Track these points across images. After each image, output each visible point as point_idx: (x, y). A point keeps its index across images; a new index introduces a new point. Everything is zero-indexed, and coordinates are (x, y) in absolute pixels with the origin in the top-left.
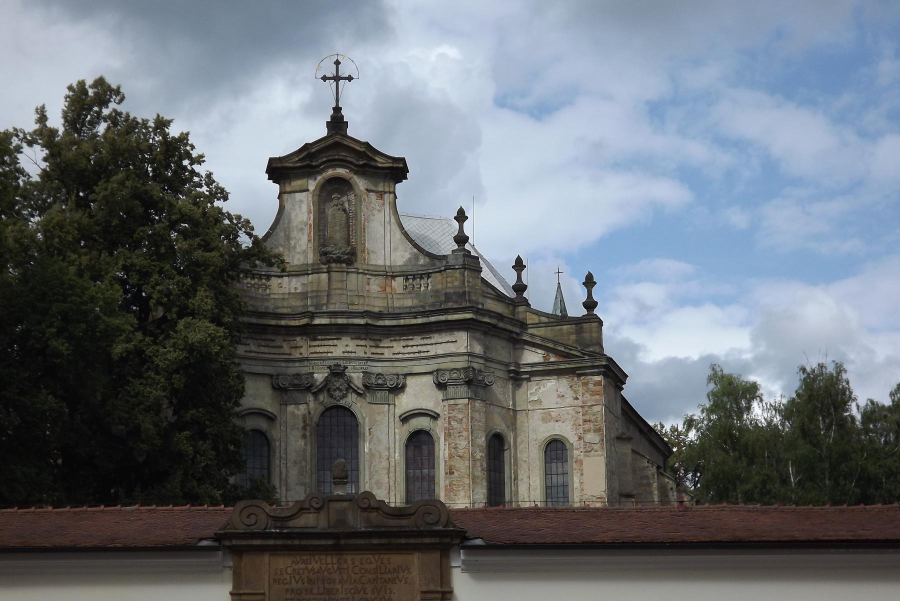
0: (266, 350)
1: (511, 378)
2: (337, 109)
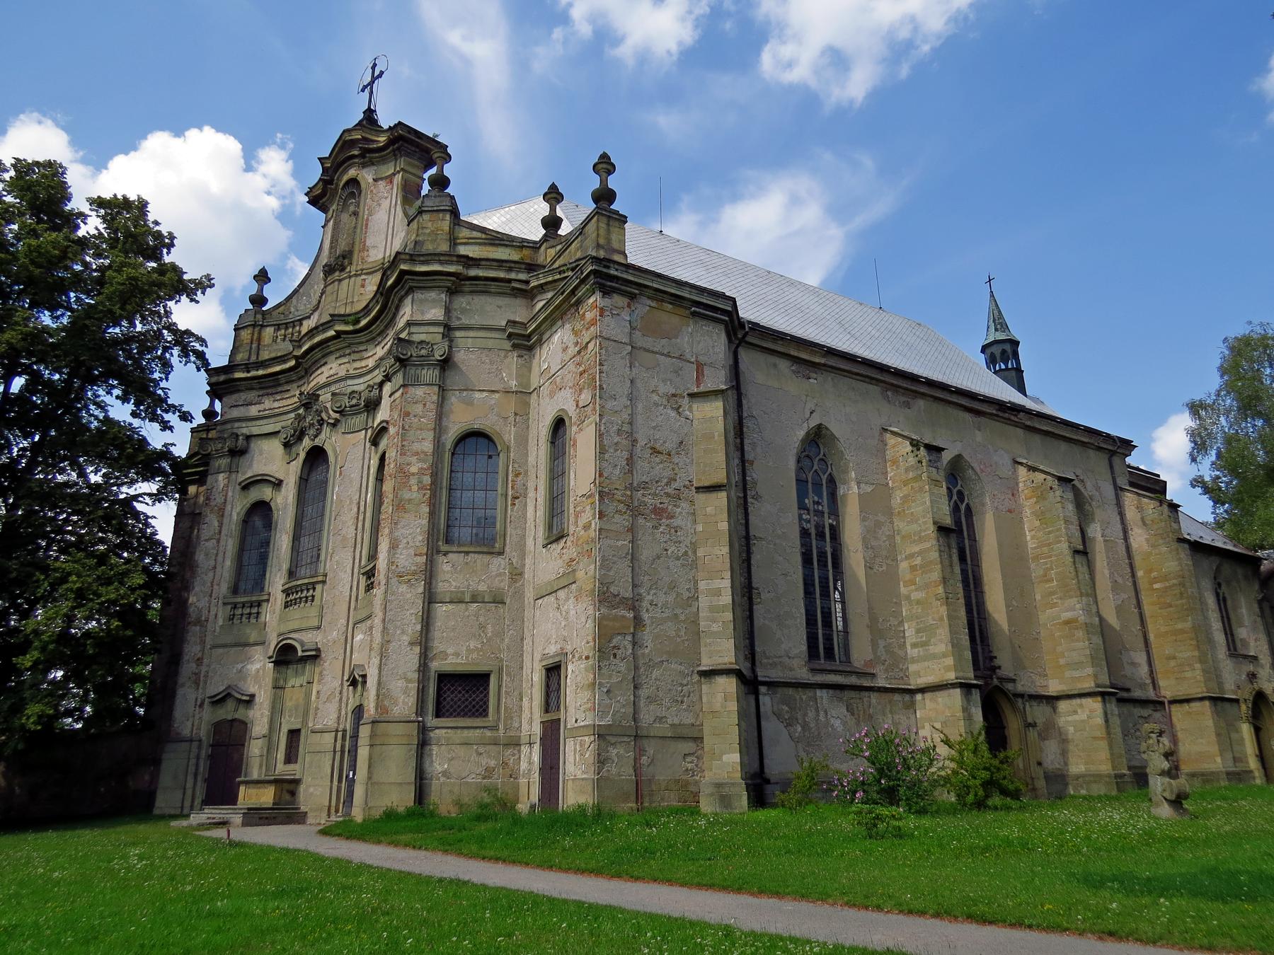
1: (515, 346)
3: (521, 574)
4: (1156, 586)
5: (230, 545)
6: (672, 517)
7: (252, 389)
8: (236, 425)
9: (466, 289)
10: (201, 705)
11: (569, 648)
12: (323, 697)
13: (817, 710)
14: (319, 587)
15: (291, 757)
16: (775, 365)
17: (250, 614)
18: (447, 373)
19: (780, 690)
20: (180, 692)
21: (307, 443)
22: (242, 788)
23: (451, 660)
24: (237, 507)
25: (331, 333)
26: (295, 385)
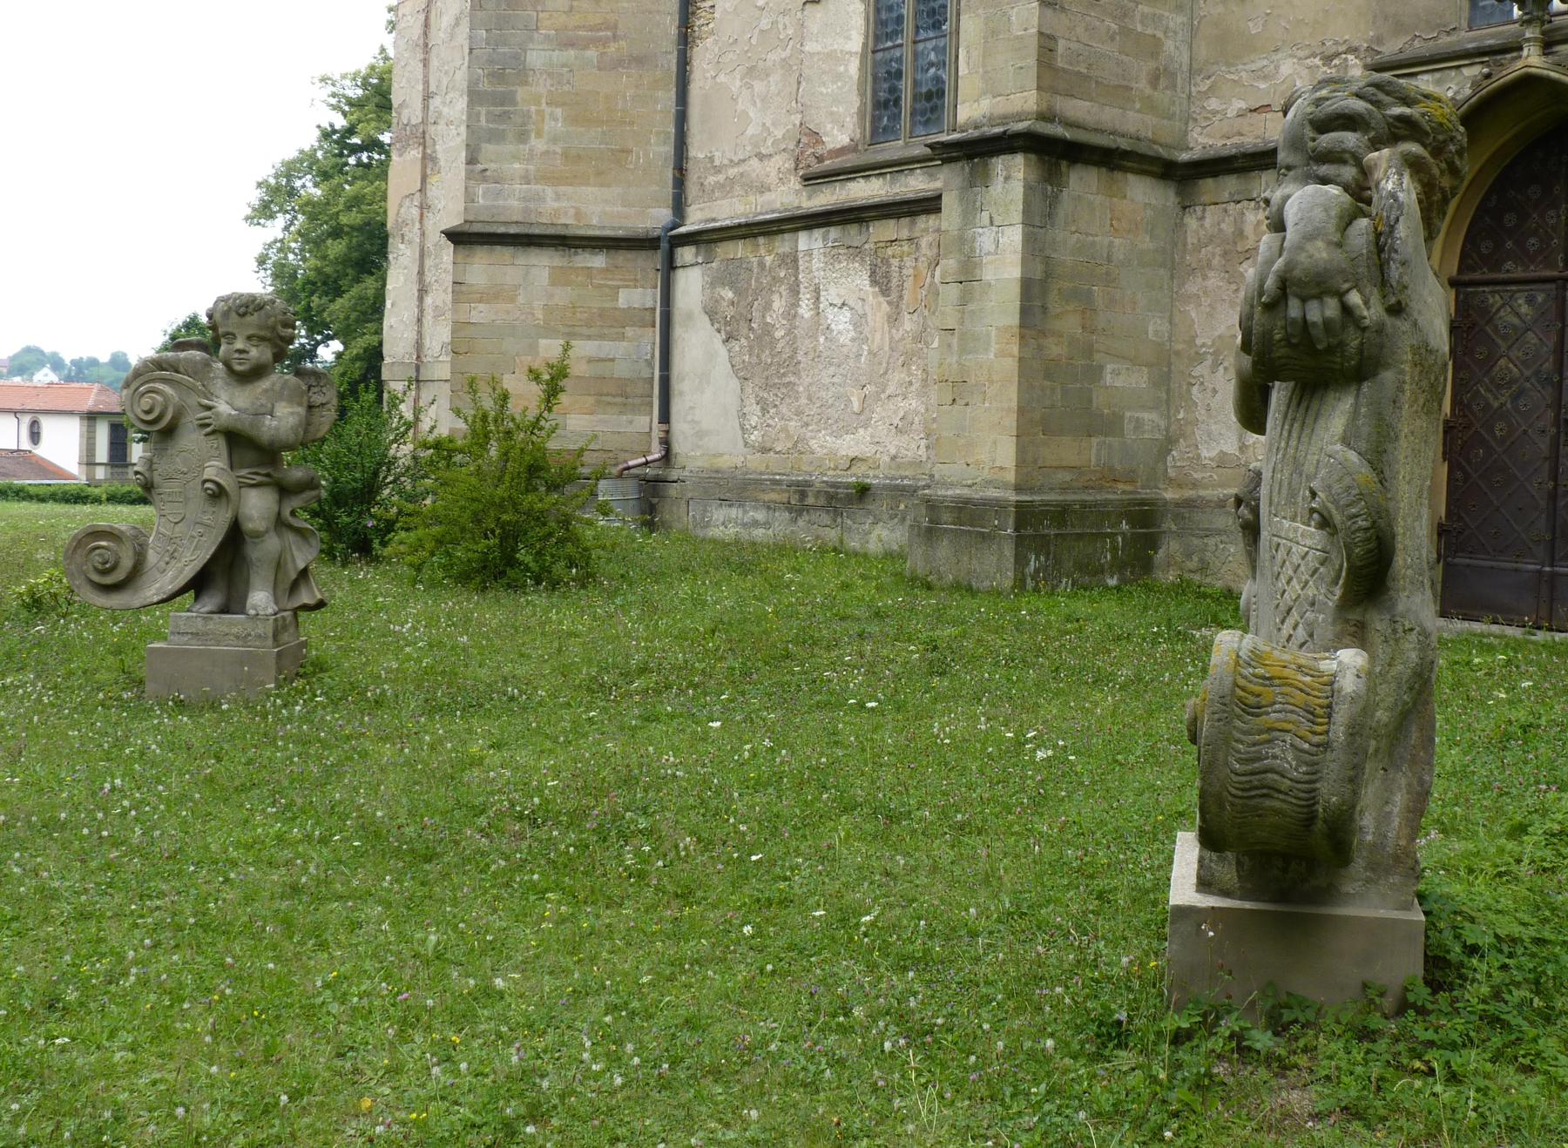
13: (795, 291)
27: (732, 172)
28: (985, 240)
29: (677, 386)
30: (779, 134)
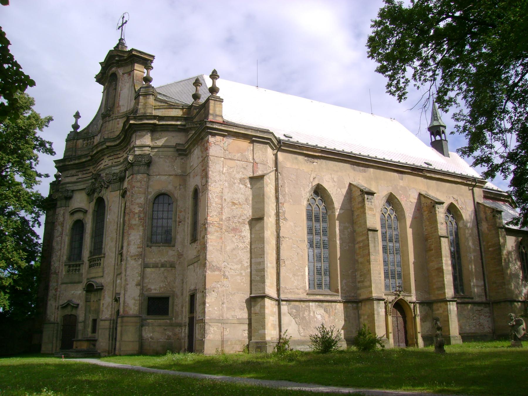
0: (86, 176)
1: (180, 155)
2: (121, 40)
3: (182, 255)
4: (490, 249)
5: (66, 239)
6: (241, 232)
7: (74, 169)
8: (68, 185)
9: (159, 130)
10: (58, 308)
11: (197, 288)
12: (105, 306)
13: (310, 311)
14: (102, 259)
15: (94, 330)
16: (296, 158)
17: (76, 269)
18: (151, 168)
19: (293, 303)
20: (49, 303)
21: (96, 195)
22: (75, 343)
23: (153, 292)
24: (69, 223)
25: (104, 146)
26: (91, 167)
27: (291, 290)
28: (380, 310)
29: (282, 326)
30: (302, 286)
